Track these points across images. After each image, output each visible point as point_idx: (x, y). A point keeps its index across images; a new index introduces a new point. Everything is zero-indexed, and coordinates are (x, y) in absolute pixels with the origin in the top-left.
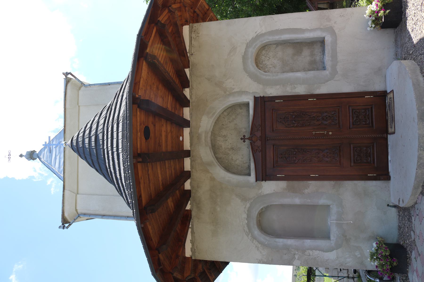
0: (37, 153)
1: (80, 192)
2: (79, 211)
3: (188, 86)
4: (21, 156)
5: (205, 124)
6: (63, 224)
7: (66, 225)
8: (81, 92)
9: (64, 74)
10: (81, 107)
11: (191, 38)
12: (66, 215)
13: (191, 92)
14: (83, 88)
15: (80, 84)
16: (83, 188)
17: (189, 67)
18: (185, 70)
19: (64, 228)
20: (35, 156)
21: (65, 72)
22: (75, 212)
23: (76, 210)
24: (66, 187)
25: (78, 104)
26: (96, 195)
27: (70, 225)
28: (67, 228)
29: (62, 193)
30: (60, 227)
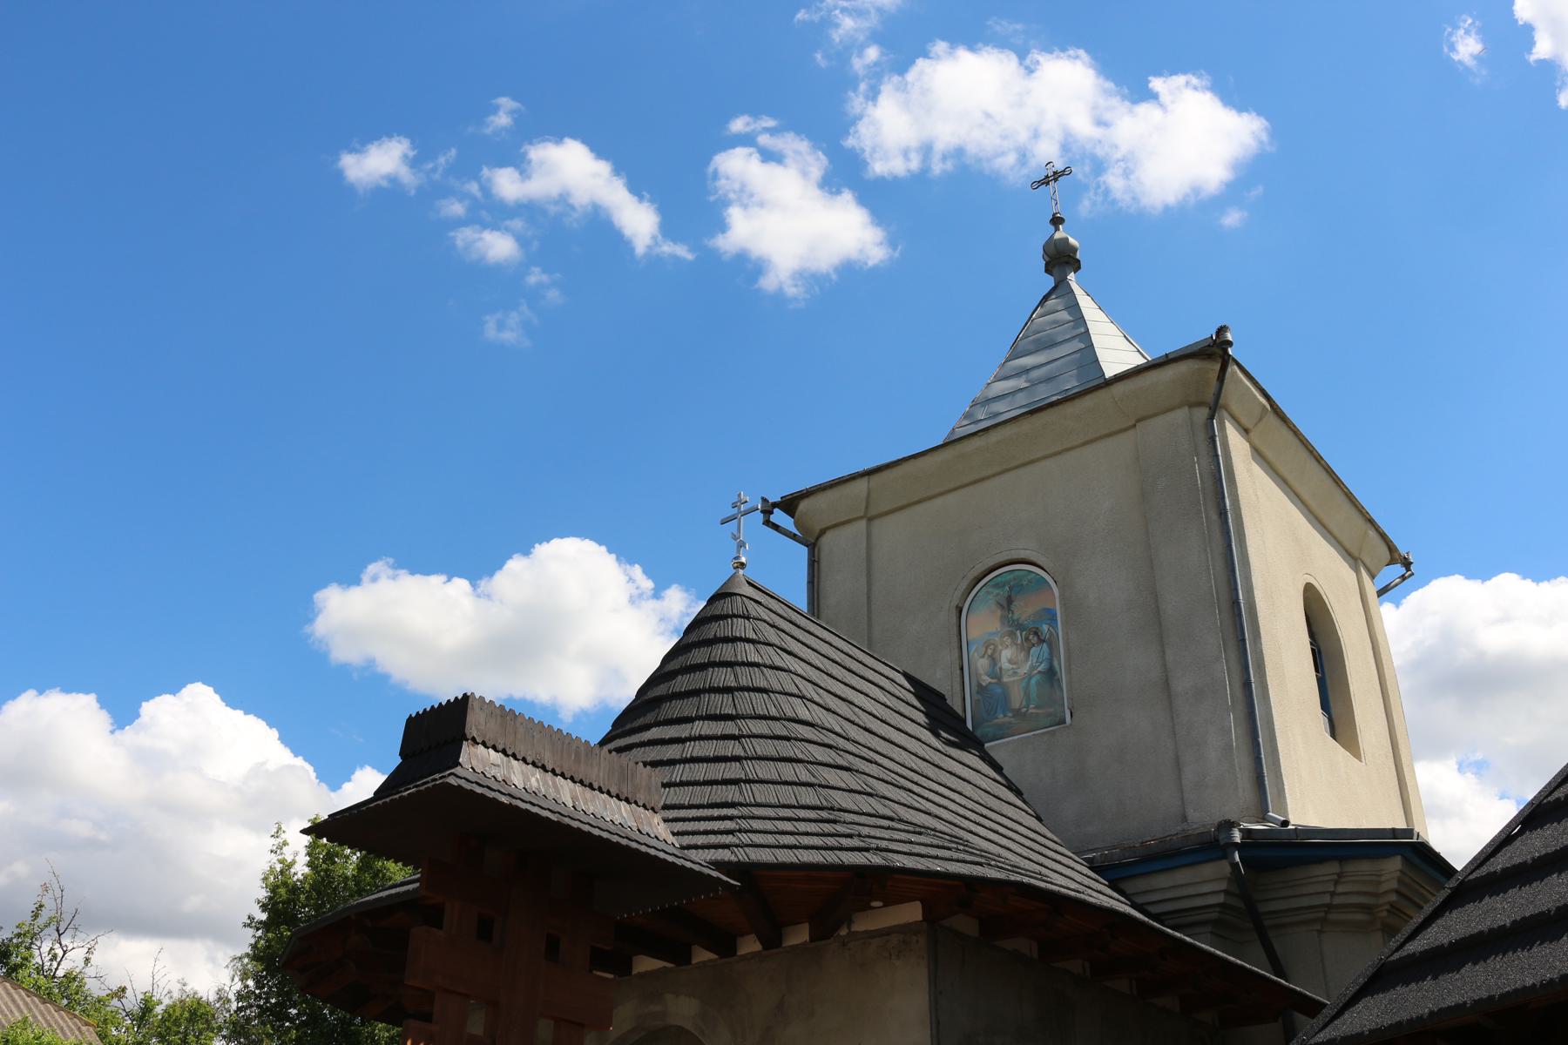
0: (1071, 276)
1: (876, 523)
2: (826, 540)
3: (766, 947)
4: (1056, 221)
5: (682, 1010)
6: (775, 505)
7: (779, 517)
8: (1181, 415)
9: (1222, 330)
10: (1131, 432)
11: (888, 934)
12: (803, 506)
13: (754, 954)
14: (1202, 413)
15: (1210, 397)
16: (891, 531)
17: (812, 940)
18: (806, 927)
19: (767, 512)
20: (1055, 271)
21: (1229, 337)
22: (817, 529)
23: (823, 532)
24: (876, 478)
25: (1139, 420)
26: (869, 584)
27: (776, 527)
28: (767, 523)
29: (860, 469)
30: (764, 500)
